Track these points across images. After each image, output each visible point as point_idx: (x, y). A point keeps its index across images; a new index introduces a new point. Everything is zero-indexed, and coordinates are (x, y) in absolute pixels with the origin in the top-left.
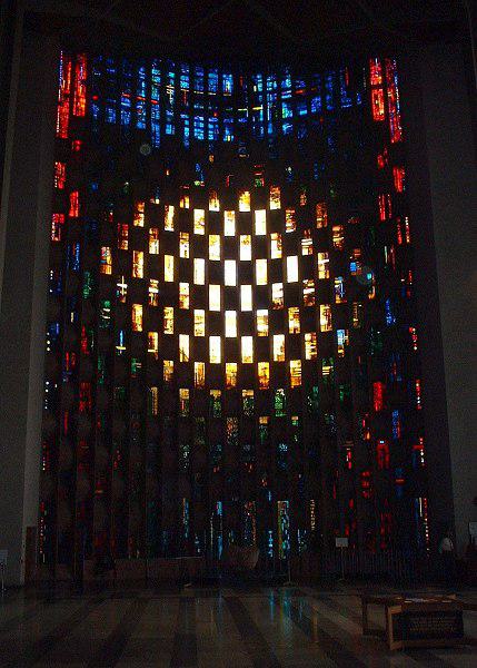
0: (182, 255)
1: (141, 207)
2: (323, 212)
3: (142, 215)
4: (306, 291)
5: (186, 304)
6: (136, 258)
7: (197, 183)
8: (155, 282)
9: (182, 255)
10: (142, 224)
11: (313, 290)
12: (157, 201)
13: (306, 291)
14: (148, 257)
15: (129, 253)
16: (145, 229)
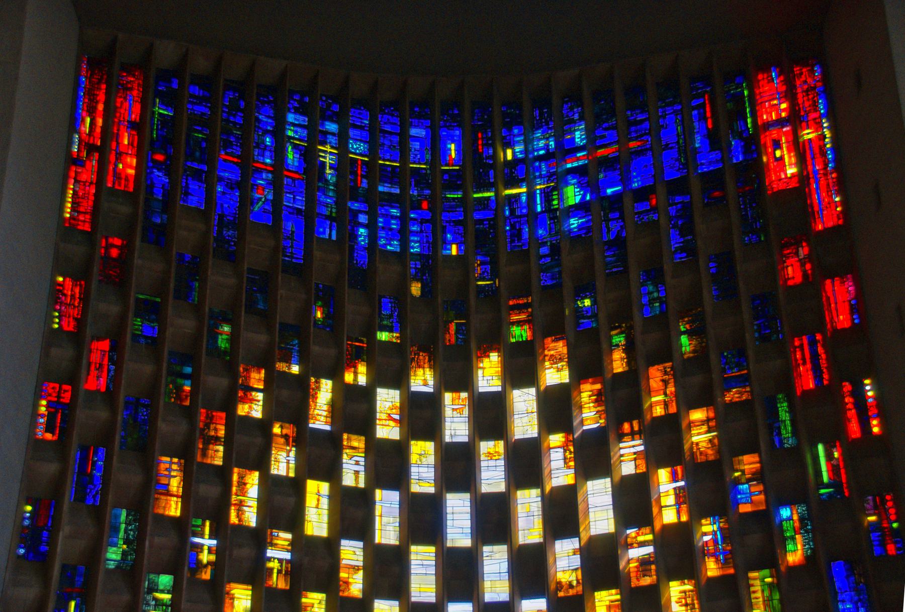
0: (348, 480)
1: (257, 379)
2: (665, 383)
3: (260, 396)
4: (635, 553)
5: (356, 586)
6: (242, 484)
7: (383, 336)
8: (284, 537)
9: (348, 480)
10: (257, 412)
11: (650, 549)
12: (295, 369)
13: (635, 553)
14: (270, 484)
15: (223, 474)
16: (264, 426)
